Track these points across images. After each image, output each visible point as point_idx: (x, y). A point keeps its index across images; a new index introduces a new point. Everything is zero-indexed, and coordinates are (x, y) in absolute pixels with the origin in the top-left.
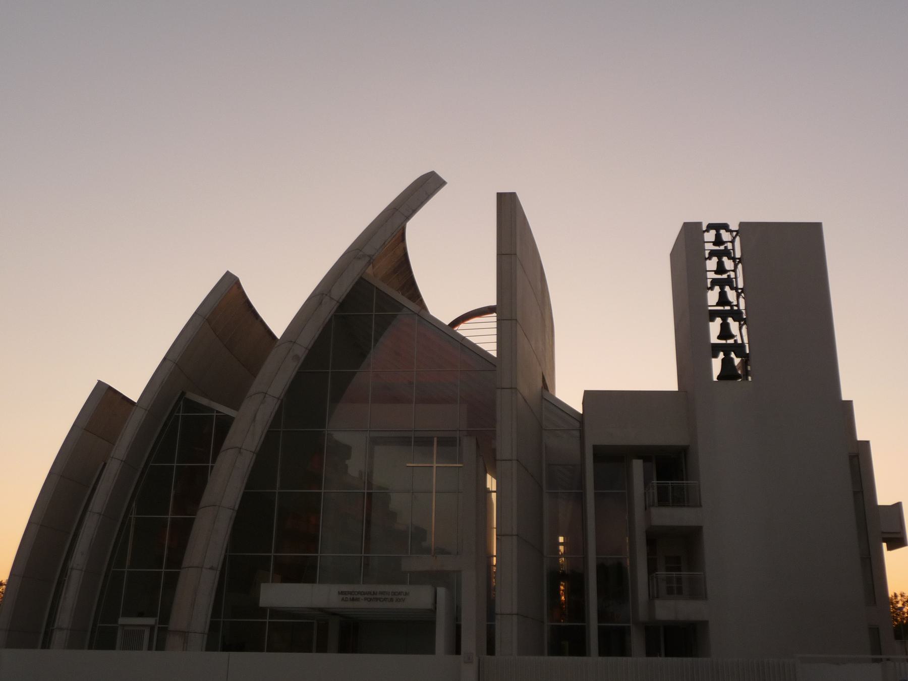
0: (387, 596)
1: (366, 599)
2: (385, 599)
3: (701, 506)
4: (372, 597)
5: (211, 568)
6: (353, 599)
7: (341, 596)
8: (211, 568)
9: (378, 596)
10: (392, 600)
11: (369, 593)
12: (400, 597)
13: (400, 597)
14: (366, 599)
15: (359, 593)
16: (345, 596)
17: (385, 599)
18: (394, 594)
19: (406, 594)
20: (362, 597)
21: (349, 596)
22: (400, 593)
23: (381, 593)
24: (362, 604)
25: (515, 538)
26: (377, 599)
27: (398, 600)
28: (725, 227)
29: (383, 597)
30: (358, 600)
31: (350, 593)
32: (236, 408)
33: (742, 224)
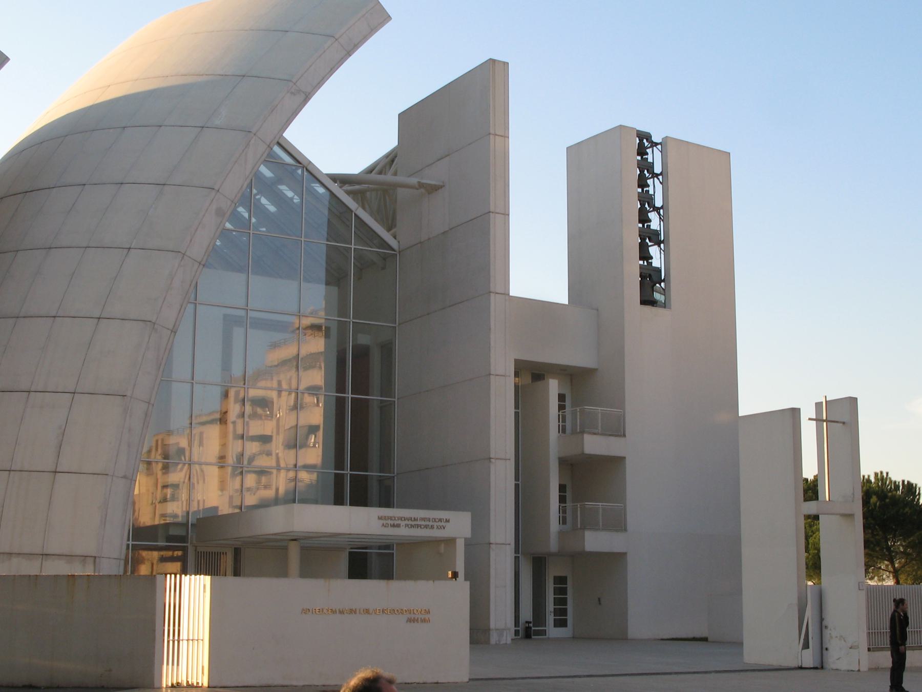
0: (427, 523)
1: (407, 525)
2: (426, 527)
3: (624, 436)
4: (413, 523)
5: (125, 477)
6: (393, 526)
7: (382, 522)
8: (125, 477)
9: (419, 523)
10: (432, 527)
12: (440, 524)
14: (407, 525)
15: (401, 519)
16: (385, 522)
18: (434, 520)
19: (448, 521)
20: (403, 523)
21: (389, 522)
22: (440, 520)
23: (423, 519)
24: (404, 532)
26: (418, 526)
28: (648, 137)
29: (423, 523)
30: (398, 526)
31: (391, 518)
33: (666, 139)
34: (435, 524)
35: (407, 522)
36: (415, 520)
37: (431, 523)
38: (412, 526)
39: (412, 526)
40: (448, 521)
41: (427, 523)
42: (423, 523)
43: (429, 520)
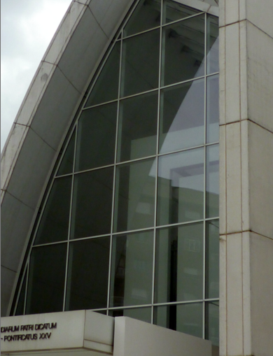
1: (6, 338)
2: (28, 337)
9: (20, 333)
10: (35, 337)
11: (10, 329)
12: (45, 331)
13: (45, 331)
17: (28, 337)
19: (54, 326)
22: (45, 326)
23: (24, 328)
25: (246, 235)
26: (19, 337)
27: (43, 337)
29: (25, 333)
32: (218, 216)
34: (39, 333)
35: (7, 334)
36: (16, 329)
37: (32, 332)
38: (12, 338)
39: (12, 338)
40: (54, 326)
41: (32, 332)
42: (25, 333)
43: (31, 327)
